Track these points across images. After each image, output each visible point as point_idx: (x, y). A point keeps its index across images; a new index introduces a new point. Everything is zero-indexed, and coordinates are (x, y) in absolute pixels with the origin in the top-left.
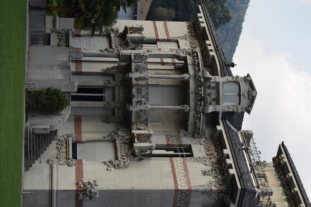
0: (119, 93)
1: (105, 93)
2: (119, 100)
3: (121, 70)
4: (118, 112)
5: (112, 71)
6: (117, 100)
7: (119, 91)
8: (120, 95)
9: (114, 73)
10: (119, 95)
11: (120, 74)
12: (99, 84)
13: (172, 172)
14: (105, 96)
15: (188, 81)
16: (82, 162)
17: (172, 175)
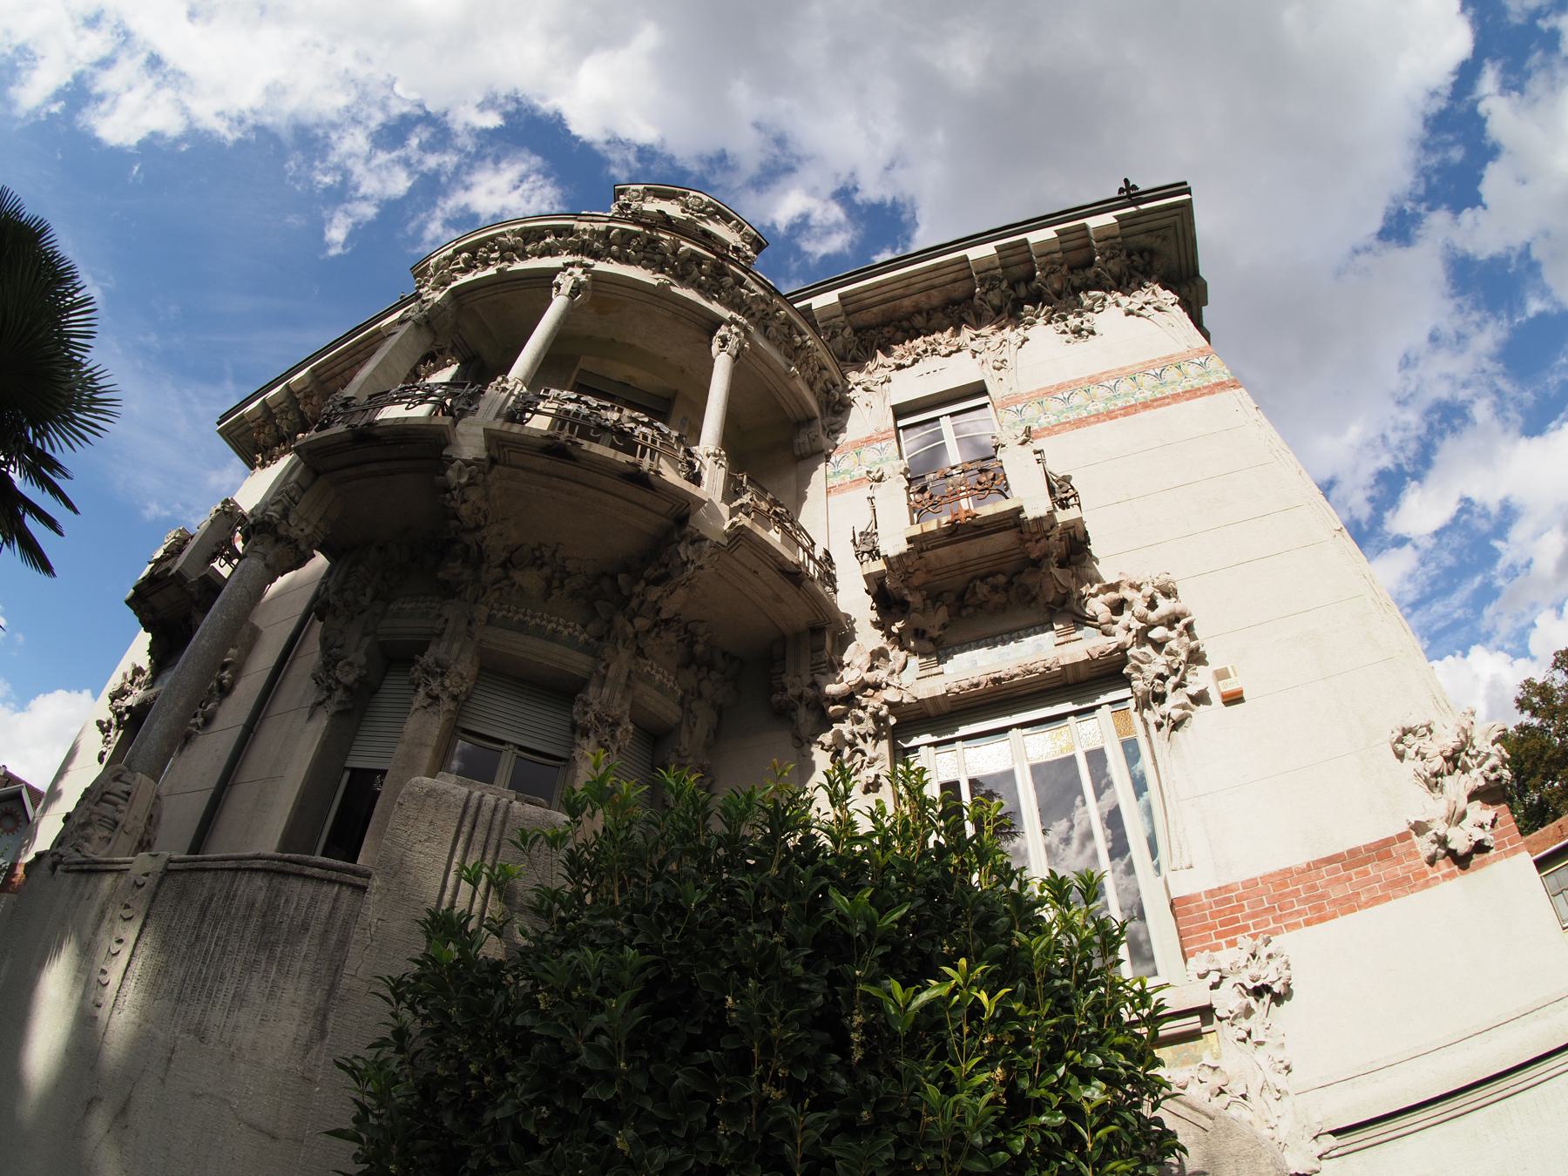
0: (539, 632)
1: (502, 742)
2: (587, 649)
3: (369, 591)
4: (660, 688)
5: (358, 653)
6: (578, 663)
7: (521, 627)
8: (554, 631)
9: (367, 640)
10: (553, 637)
11: (393, 607)
12: (422, 745)
13: (1121, 419)
14: (522, 748)
15: (598, 278)
16: (1210, 893)
17: (1145, 415)
